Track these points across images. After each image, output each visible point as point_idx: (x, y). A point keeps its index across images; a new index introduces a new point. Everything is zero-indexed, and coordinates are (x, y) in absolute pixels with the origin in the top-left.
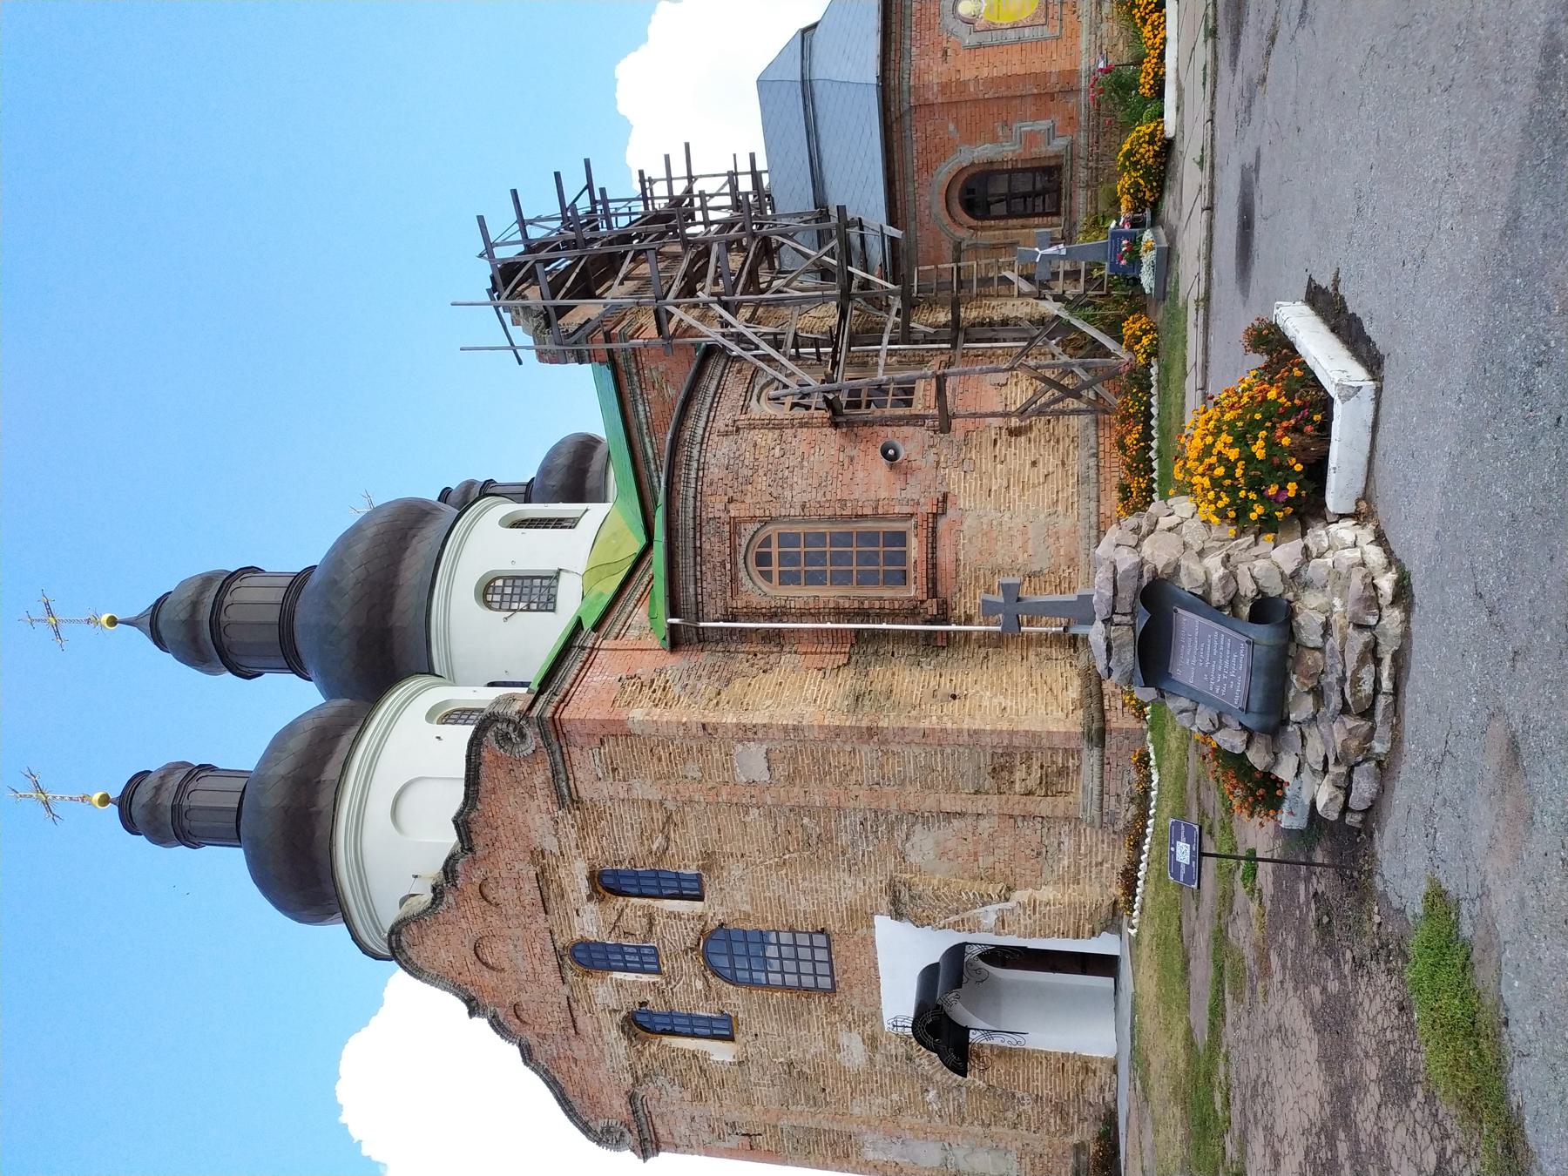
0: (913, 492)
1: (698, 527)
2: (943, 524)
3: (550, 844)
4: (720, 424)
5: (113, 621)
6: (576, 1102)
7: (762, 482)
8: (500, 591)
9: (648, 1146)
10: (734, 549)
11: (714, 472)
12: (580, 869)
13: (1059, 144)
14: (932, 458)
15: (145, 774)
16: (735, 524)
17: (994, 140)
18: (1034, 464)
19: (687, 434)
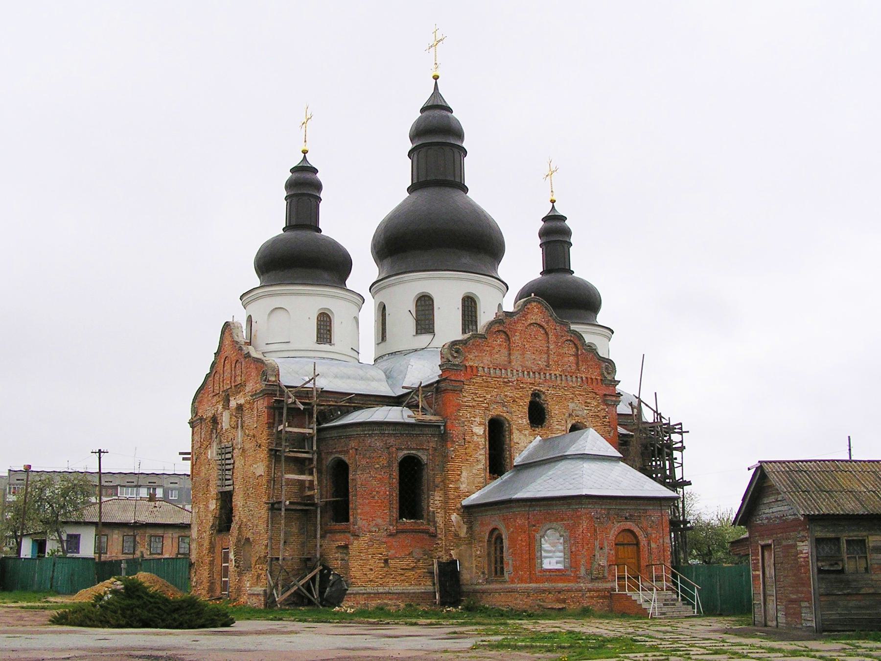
0: (360, 523)
1: (349, 437)
2: (349, 535)
3: (248, 389)
4: (391, 441)
5: (436, 78)
6: (200, 395)
7: (364, 462)
8: (425, 304)
9: (192, 424)
10: (340, 452)
11: (369, 441)
12: (242, 401)
13: (506, 575)
14: (374, 529)
15: (315, 171)
16: (347, 452)
17: (509, 548)
18: (371, 570)
19: (384, 427)
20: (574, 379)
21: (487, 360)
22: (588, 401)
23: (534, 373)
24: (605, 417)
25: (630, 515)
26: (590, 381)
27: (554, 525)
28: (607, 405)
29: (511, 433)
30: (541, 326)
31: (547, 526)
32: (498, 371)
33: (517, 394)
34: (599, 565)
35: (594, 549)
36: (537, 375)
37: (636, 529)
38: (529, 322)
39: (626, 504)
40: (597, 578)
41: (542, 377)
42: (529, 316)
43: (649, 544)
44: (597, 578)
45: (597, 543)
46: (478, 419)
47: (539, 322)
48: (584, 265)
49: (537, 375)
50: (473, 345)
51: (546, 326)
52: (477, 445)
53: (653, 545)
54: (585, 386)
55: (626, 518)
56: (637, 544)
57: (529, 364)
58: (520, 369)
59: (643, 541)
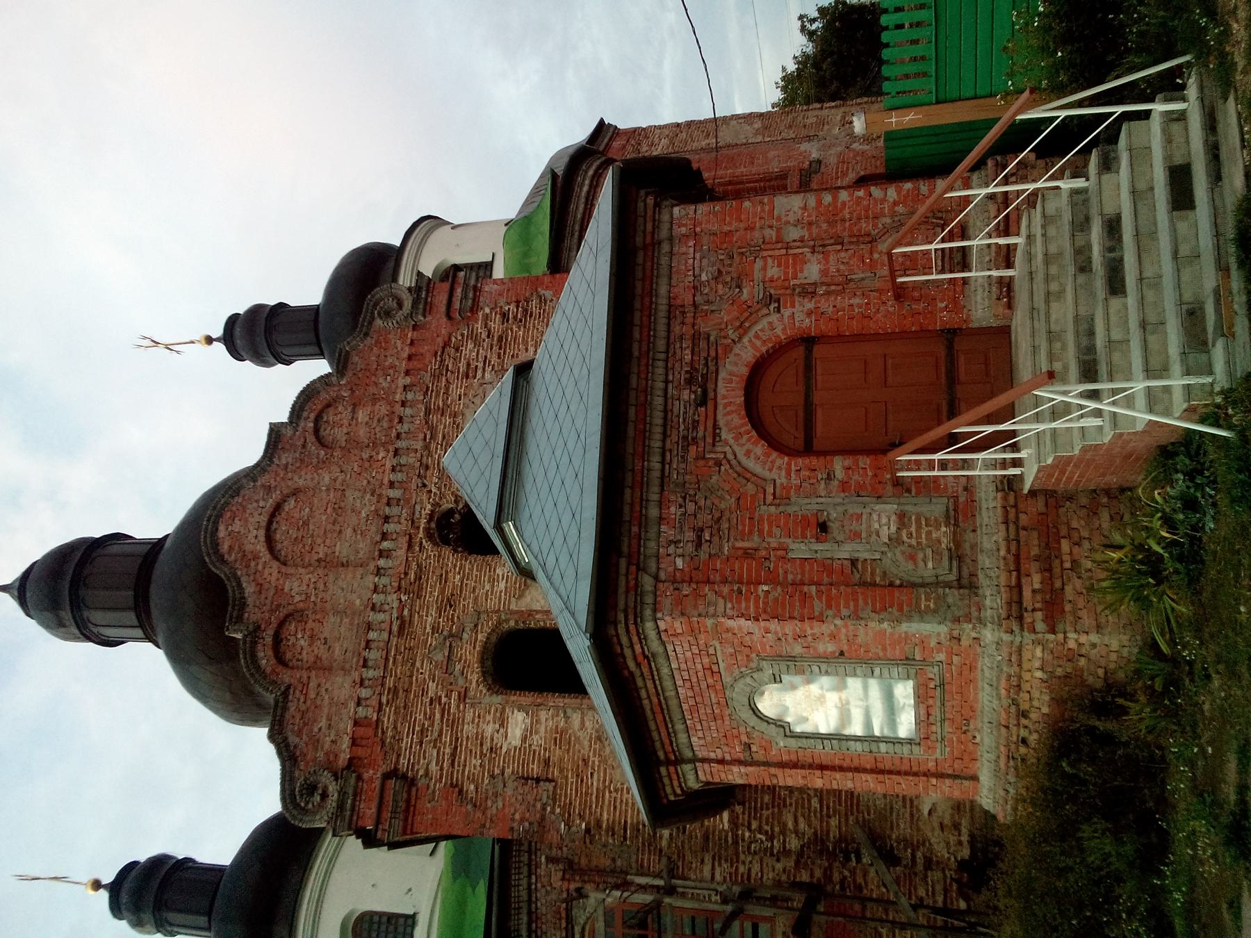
20: (408, 411)
21: (341, 687)
22: (462, 366)
23: (384, 536)
24: (505, 316)
25: (690, 382)
26: (414, 364)
27: (737, 695)
28: (475, 308)
29: (531, 613)
30: (278, 508)
31: (746, 714)
32: (374, 655)
33: (432, 594)
34: (895, 541)
35: (826, 566)
36: (390, 527)
37: (745, 354)
38: (261, 548)
39: (645, 406)
40: (957, 555)
41: (395, 510)
42: (248, 547)
43: (808, 291)
44: (957, 555)
45: (800, 549)
46: (489, 729)
47: (264, 519)
48: (306, 288)
49: (390, 527)
50: (299, 733)
51: (276, 496)
52: (560, 737)
53: (812, 271)
54: (427, 378)
55: (702, 401)
56: (808, 341)
57: (364, 546)
58: (371, 580)
59: (797, 317)
